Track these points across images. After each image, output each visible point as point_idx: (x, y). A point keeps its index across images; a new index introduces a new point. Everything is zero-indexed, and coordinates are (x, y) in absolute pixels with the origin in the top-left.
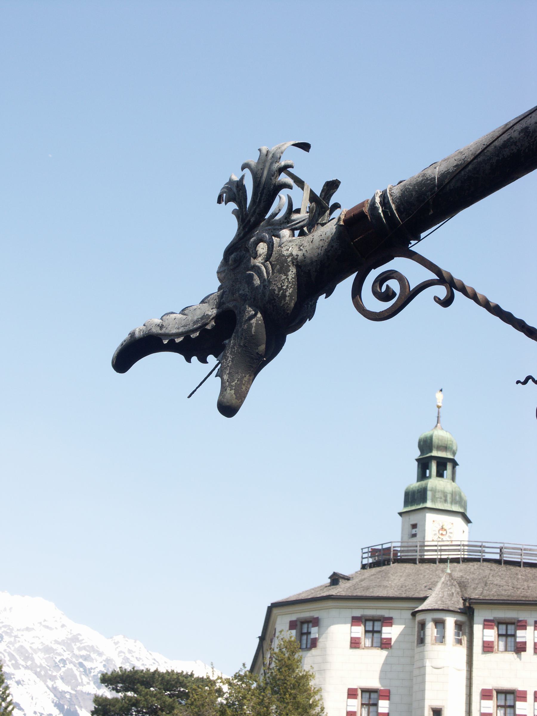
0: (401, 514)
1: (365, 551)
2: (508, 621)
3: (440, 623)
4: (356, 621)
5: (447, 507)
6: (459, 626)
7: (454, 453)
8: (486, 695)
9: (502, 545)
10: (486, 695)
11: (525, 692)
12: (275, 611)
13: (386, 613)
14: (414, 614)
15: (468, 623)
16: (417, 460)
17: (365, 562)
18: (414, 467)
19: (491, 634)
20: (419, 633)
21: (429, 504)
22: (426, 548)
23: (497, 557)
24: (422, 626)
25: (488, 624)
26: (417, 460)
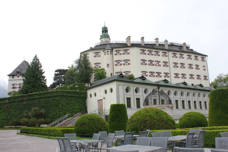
0: (100, 39)
4: (94, 53)
5: (107, 37)
6: (111, 52)
7: (107, 29)
8: (116, 61)
10: (116, 61)
11: (121, 60)
12: (82, 53)
13: (99, 52)
14: (104, 51)
16: (102, 31)
18: (101, 32)
19: (116, 53)
23: (115, 43)
24: (105, 52)
25: (115, 51)
26: (102, 31)
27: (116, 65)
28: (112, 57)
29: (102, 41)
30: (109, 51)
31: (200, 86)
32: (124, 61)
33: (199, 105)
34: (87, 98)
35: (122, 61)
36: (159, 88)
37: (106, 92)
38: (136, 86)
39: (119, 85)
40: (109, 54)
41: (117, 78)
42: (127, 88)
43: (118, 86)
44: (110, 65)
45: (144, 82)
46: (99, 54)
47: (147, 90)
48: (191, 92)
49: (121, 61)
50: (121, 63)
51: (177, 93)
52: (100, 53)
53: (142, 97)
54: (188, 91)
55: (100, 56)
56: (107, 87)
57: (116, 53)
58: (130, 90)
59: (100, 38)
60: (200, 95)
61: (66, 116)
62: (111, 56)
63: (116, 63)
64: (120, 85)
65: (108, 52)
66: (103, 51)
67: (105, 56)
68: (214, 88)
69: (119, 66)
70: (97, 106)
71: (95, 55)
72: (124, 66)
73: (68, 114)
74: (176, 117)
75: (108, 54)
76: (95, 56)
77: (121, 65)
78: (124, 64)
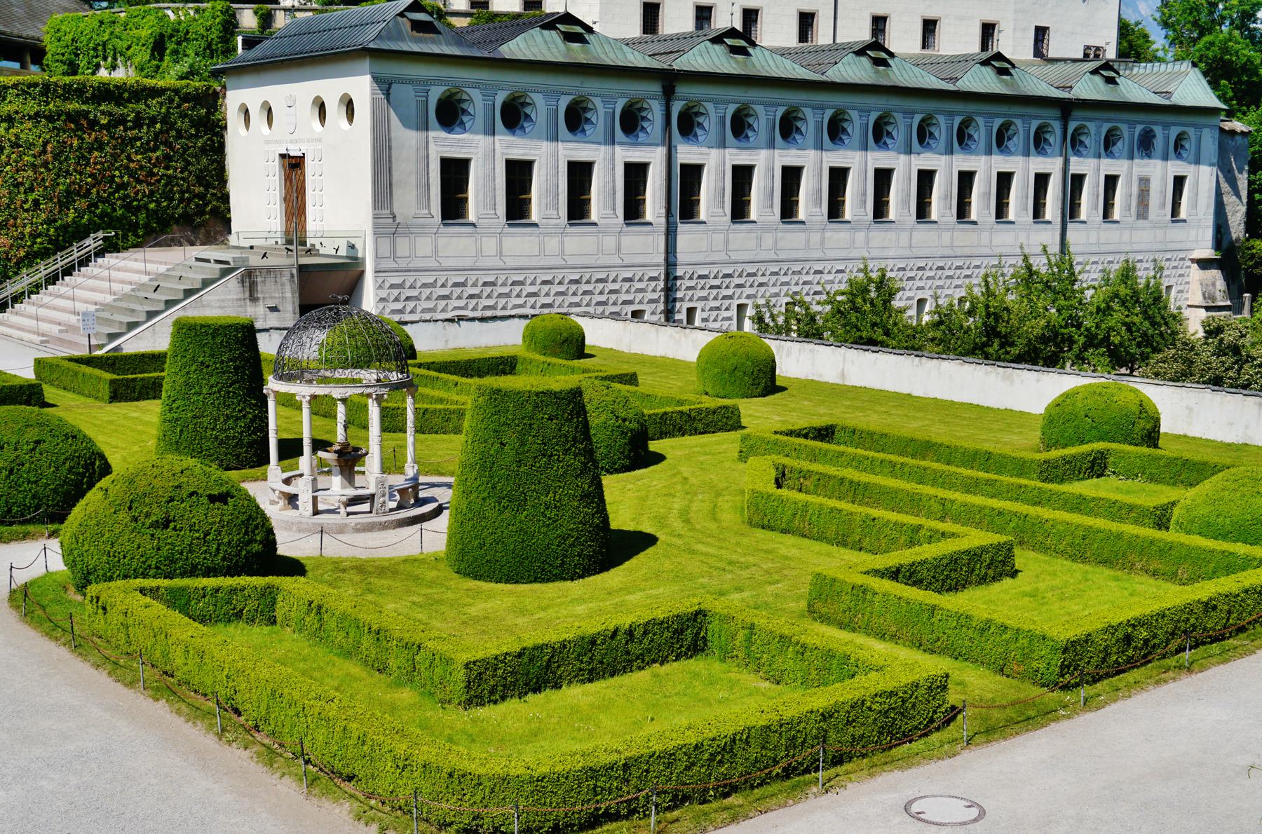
31: (988, 72)
33: (947, 197)
34: (225, 128)
36: (668, 95)
37: (322, 109)
38: (506, 85)
39: (390, 85)
41: (379, 36)
42: (450, 96)
43: (389, 88)
45: (576, 52)
47: (590, 106)
48: (909, 113)
51: (804, 119)
54: (879, 104)
56: (331, 87)
58: (471, 110)
60: (971, 131)
61: (91, 243)
64: (402, 82)
68: (1097, 78)
70: (277, 192)
73: (100, 234)
74: (777, 274)
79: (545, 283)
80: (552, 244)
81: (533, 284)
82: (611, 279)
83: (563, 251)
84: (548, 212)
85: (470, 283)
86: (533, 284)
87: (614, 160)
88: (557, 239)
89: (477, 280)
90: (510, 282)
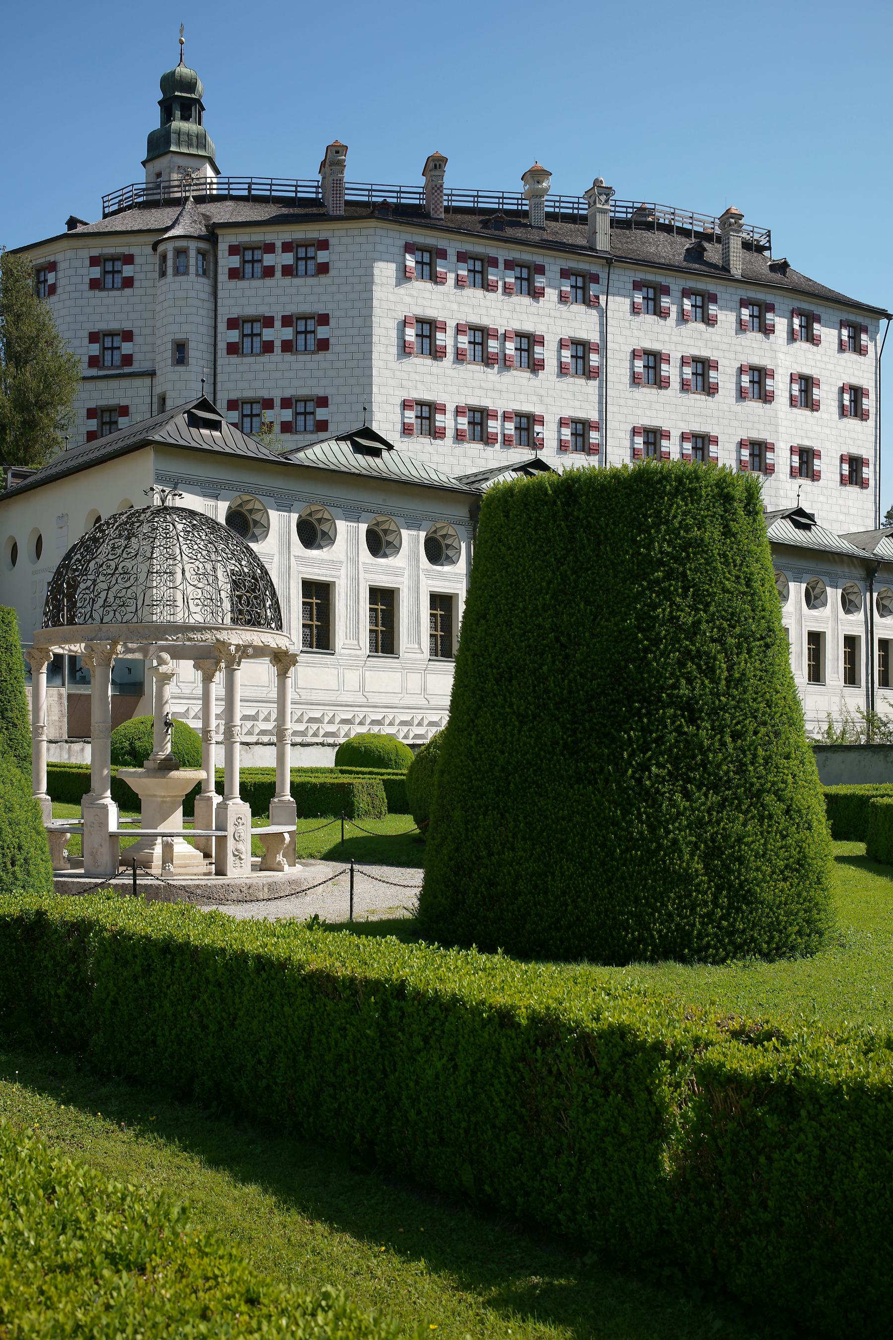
0: (144, 163)
1: (105, 199)
2: (254, 245)
3: (181, 253)
4: (94, 261)
5: (193, 151)
9: (249, 180)
10: (232, 324)
13: (126, 251)
14: (155, 247)
15: (212, 251)
17: (107, 211)
19: (235, 262)
20: (161, 266)
21: (173, 148)
22: (172, 190)
24: (164, 258)
25: (233, 250)
27: (233, 349)
28: (208, 289)
29: (159, 175)
30: (193, 246)
32: (287, 321)
35: (278, 323)
40: (186, 273)
44: (197, 353)
46: (128, 271)
49: (268, 322)
50: (268, 334)
52: (129, 259)
53: (343, 572)
55: (128, 282)
57: (235, 262)
59: (144, 157)
62: (202, 285)
63: (234, 336)
65: (182, 258)
66: (149, 250)
67: (163, 281)
69: (251, 359)
71: (96, 272)
72: (288, 357)
75: (182, 269)
76: (95, 284)
77: (268, 347)
78: (287, 347)
79: (344, 722)
80: (352, 678)
81: (331, 722)
82: (416, 722)
83: (364, 687)
84: (347, 642)
85: (262, 716)
86: (331, 722)
87: (418, 588)
88: (357, 673)
89: (269, 714)
90: (306, 718)
